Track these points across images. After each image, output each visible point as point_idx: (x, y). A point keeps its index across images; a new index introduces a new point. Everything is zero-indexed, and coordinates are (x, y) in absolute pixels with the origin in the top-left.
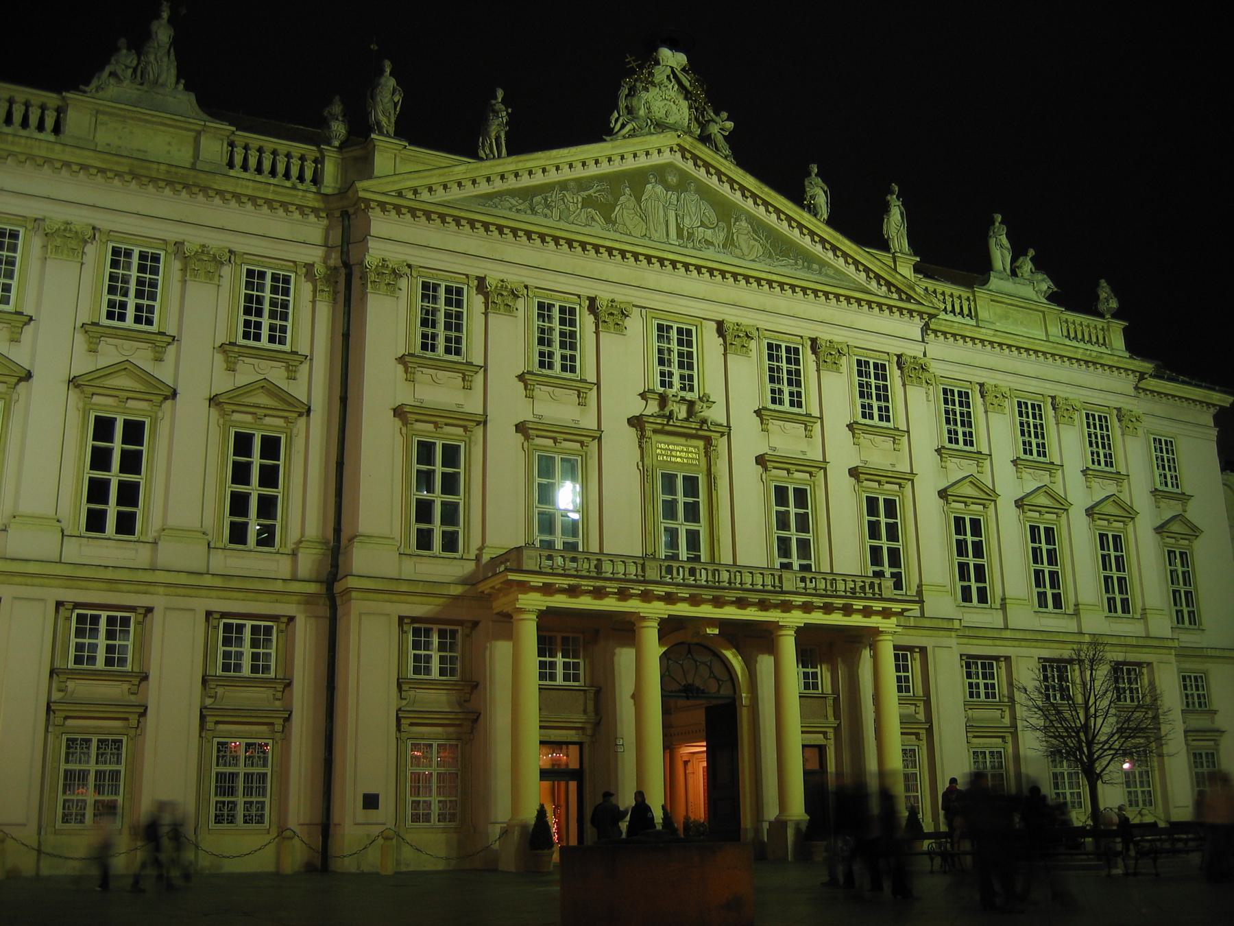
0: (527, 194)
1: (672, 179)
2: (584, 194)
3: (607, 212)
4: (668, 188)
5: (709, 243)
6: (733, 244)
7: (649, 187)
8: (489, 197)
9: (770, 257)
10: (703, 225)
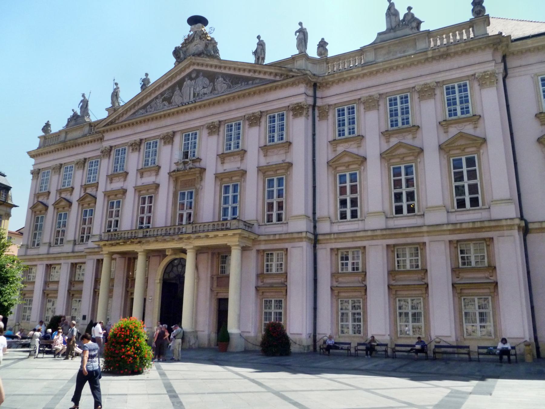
0: (144, 107)
1: (194, 75)
2: (163, 97)
3: (168, 100)
4: (191, 79)
5: (205, 94)
6: (215, 90)
7: (185, 83)
8: (134, 113)
9: (230, 87)
10: (204, 88)
